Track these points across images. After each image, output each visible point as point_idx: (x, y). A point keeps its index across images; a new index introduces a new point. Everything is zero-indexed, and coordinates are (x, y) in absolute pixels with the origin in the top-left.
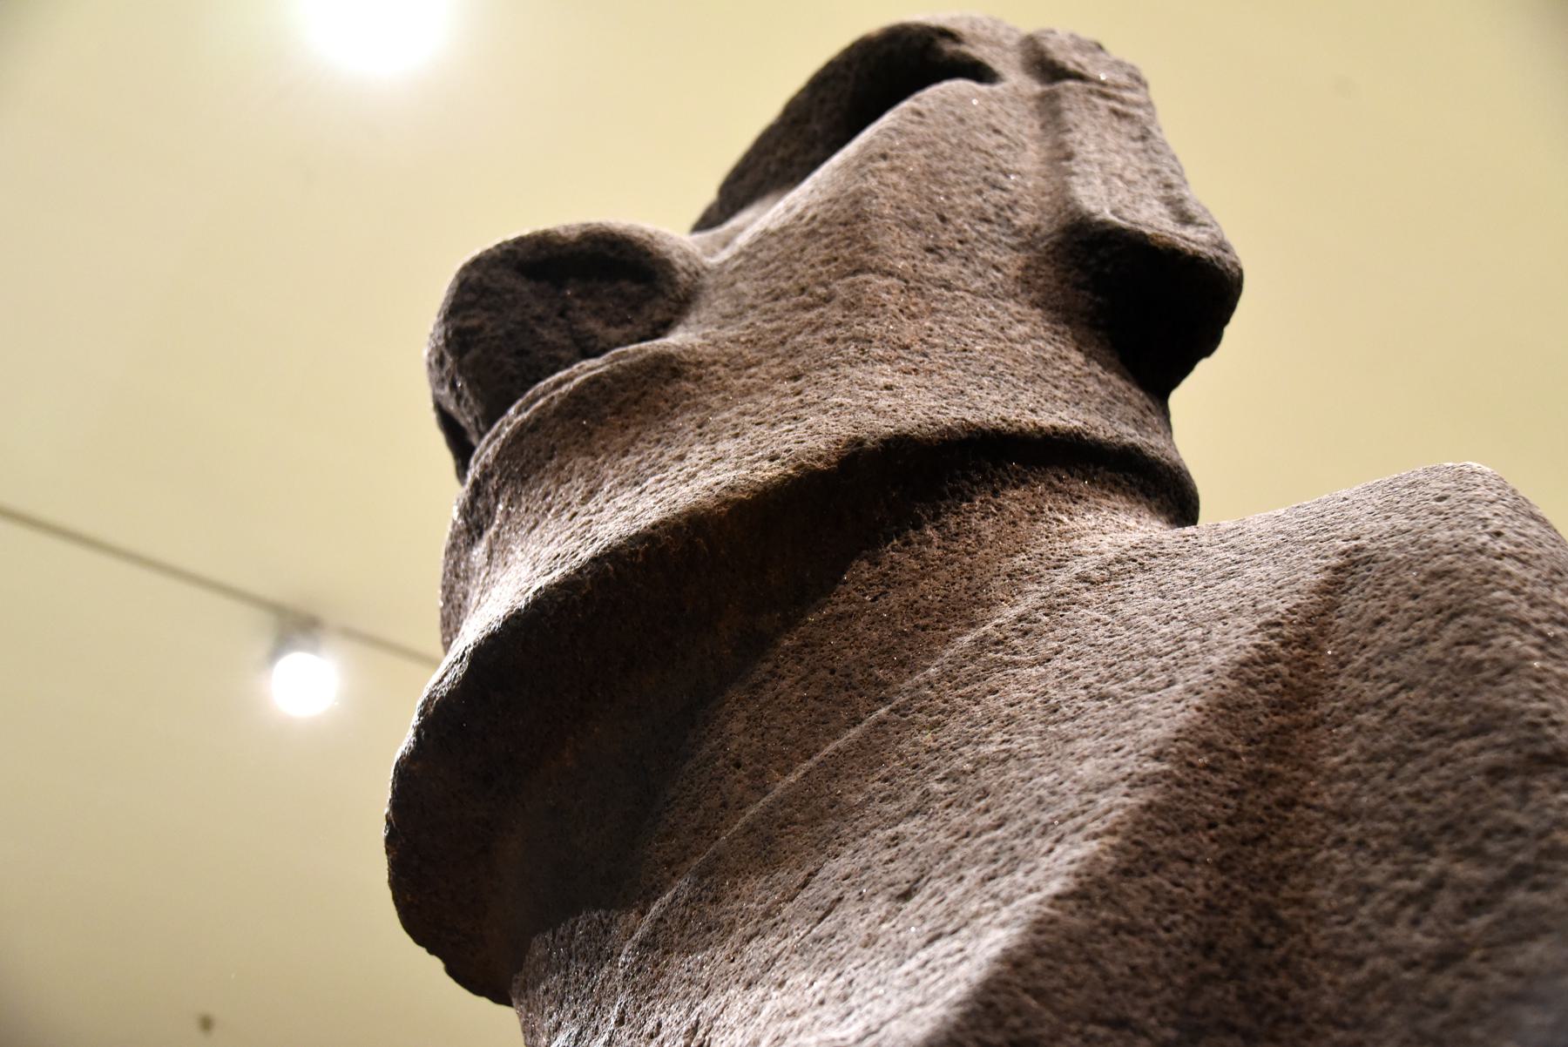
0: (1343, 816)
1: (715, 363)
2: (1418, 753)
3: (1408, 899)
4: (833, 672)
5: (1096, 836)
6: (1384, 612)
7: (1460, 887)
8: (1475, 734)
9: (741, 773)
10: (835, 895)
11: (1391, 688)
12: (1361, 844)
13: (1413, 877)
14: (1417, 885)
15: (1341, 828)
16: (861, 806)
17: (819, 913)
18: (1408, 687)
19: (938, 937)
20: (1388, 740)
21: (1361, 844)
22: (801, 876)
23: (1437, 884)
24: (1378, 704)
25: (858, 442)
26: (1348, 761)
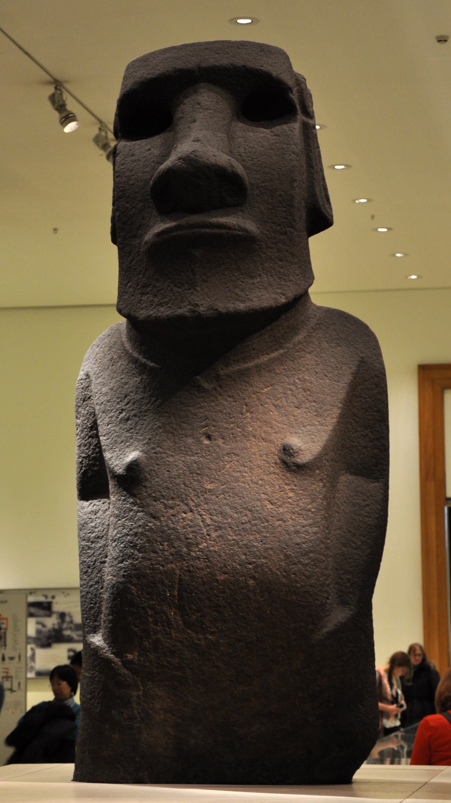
0: (355, 415)
1: (262, 241)
3: (362, 435)
4: (274, 337)
5: (334, 418)
6: (367, 379)
9: (254, 352)
10: (279, 396)
11: (367, 396)
12: (357, 422)
13: (364, 432)
14: (364, 434)
15: (355, 417)
16: (279, 374)
18: (369, 398)
19: (309, 425)
21: (357, 422)
23: (367, 435)
25: (296, 296)
26: (358, 406)
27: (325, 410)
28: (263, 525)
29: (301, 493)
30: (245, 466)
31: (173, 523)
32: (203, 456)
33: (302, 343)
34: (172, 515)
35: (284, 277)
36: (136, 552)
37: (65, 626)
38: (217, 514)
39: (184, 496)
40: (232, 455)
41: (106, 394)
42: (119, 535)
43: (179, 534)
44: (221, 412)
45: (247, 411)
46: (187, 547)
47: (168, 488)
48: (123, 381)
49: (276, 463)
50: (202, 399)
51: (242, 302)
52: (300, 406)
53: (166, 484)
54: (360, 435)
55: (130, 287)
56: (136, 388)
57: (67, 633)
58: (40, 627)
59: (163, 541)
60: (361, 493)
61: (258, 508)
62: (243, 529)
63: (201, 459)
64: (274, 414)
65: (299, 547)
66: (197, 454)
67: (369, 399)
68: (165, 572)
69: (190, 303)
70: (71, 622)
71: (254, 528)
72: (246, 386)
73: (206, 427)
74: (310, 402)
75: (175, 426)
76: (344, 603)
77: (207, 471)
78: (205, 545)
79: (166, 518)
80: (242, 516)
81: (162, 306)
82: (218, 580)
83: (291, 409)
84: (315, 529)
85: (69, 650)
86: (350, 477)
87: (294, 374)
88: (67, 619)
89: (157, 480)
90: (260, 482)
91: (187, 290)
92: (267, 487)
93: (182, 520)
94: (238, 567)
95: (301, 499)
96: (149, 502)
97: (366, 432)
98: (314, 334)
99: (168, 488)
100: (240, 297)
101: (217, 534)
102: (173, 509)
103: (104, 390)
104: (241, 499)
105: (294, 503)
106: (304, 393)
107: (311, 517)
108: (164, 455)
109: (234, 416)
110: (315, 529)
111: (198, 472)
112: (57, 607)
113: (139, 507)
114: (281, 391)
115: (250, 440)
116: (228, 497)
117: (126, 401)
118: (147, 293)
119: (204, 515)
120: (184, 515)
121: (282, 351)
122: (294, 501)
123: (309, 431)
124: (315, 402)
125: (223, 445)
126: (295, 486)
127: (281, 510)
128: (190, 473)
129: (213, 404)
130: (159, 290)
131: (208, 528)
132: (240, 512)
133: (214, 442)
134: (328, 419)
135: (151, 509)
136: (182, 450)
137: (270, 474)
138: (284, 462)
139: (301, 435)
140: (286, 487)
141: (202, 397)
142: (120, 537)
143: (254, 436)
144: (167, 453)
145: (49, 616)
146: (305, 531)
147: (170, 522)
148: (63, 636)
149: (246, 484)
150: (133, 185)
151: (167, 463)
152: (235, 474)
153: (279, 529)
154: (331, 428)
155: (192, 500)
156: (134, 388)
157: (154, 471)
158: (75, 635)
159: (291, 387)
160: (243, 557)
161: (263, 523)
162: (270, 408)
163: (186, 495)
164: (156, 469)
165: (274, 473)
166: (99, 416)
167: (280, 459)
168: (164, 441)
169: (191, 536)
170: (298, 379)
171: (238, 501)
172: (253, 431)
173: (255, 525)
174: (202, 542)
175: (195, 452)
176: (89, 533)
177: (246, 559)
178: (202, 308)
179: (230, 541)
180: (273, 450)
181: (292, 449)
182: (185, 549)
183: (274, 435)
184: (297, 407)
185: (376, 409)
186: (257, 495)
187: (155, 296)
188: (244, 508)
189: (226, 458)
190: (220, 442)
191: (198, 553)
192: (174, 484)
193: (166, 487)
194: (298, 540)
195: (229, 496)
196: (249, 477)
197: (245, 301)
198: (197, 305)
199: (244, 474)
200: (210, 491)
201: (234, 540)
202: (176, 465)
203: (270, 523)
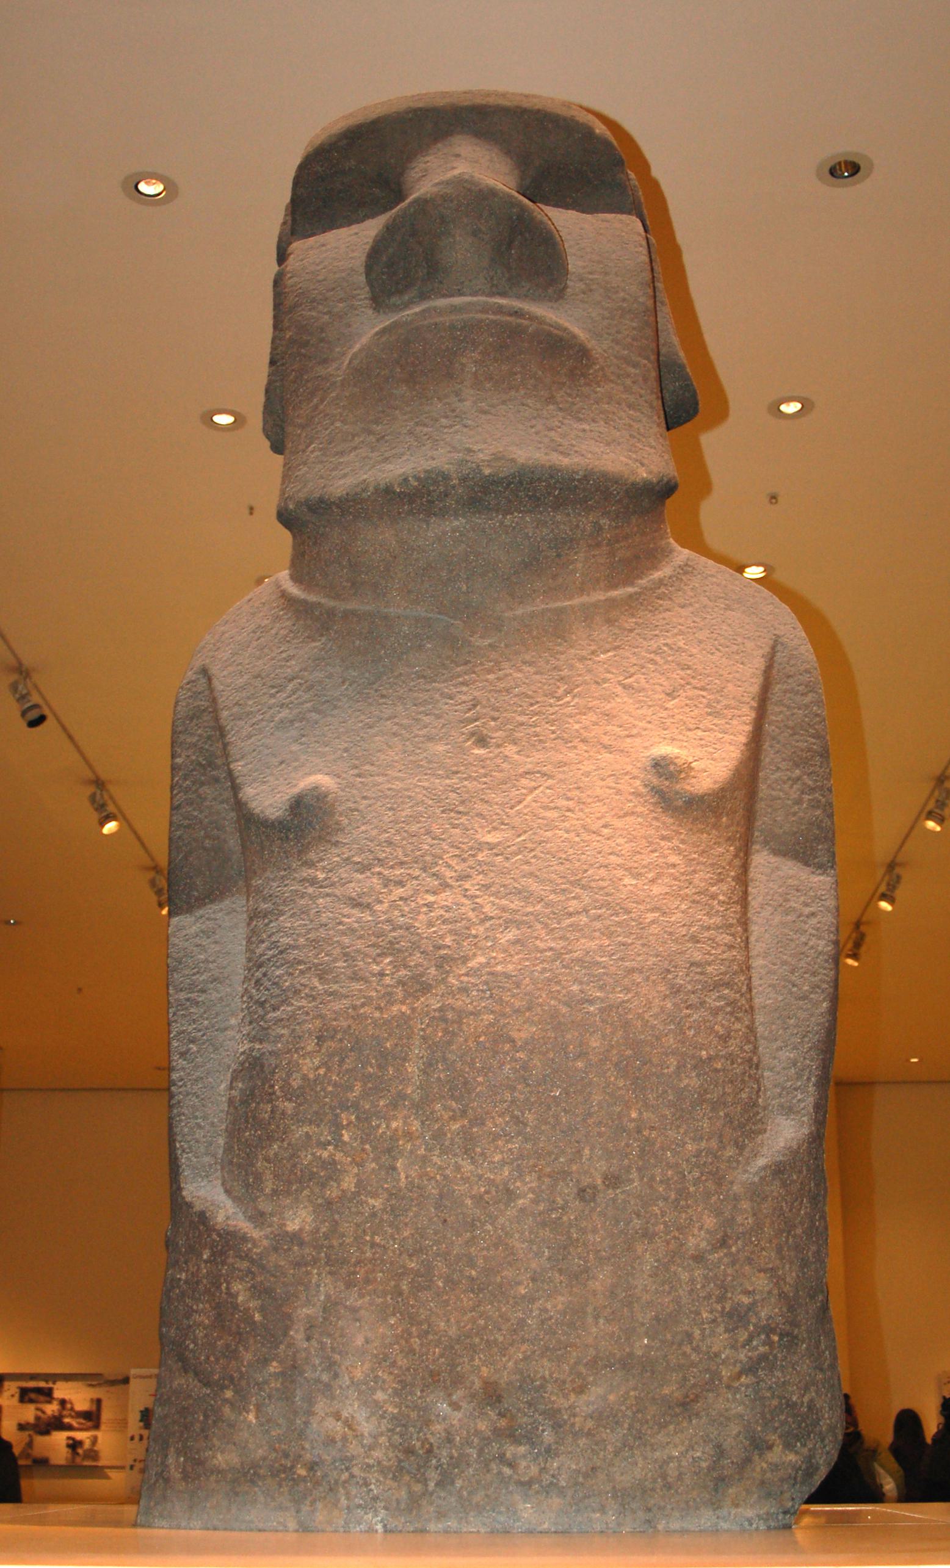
2: (798, 734)
5: (746, 724)
7: (805, 784)
8: (814, 738)
10: (632, 670)
17: (628, 675)
18: (799, 709)
19: (698, 728)
20: (790, 723)
22: (608, 646)
23: (798, 779)
24: (788, 707)
26: (777, 721)
27: (727, 707)
28: (617, 919)
29: (694, 859)
30: (569, 799)
31: (402, 916)
32: (470, 777)
33: (666, 585)
34: (401, 899)
35: (641, 438)
36: (316, 982)
37: (65, 1413)
38: (507, 894)
39: (428, 858)
40: (538, 775)
41: (243, 688)
42: (271, 953)
43: (416, 938)
44: (508, 691)
45: (567, 692)
46: (439, 967)
47: (389, 843)
48: (284, 655)
49: (638, 794)
50: (467, 667)
51: (565, 454)
52: (676, 694)
53: (387, 835)
54: (786, 778)
55: (312, 452)
56: (314, 660)
57: (67, 1420)
58: (39, 1413)
59: (378, 955)
60: (798, 890)
61: (604, 884)
62: (571, 926)
63: (466, 783)
64: (623, 702)
65: (699, 970)
66: (457, 772)
67: (796, 711)
68: (386, 1022)
69: (454, 447)
70: (72, 1409)
71: (598, 925)
72: (560, 645)
73: (476, 720)
74: (696, 688)
75: (405, 722)
76: (789, 1110)
77: (479, 807)
78: (482, 960)
79: (386, 905)
80: (568, 899)
81: (390, 463)
82: (513, 1041)
83: (656, 696)
84: (728, 939)
85: (69, 1438)
86: (774, 860)
87: (656, 635)
88: (69, 1406)
89: (363, 828)
90: (606, 831)
91: (446, 427)
92: (621, 841)
93: (425, 909)
94: (564, 1010)
95: (695, 872)
96: (344, 876)
97: (798, 772)
98: (684, 578)
99: (391, 843)
100: (560, 445)
101: (511, 934)
102: (403, 886)
103: (241, 681)
104: (562, 863)
105: (683, 878)
106: (682, 673)
107: (718, 911)
108: (380, 779)
109: (539, 700)
110: (728, 939)
111: (461, 809)
112: (58, 1394)
113: (321, 887)
114: (635, 662)
115: (575, 747)
116: (533, 860)
117: (290, 686)
118: (355, 448)
119: (477, 897)
120: (431, 898)
121: (630, 590)
122: (683, 874)
123: (701, 739)
124: (703, 689)
125: (516, 757)
126: (683, 842)
127: (656, 890)
128: (443, 812)
129: (491, 677)
130: (383, 437)
131: (488, 924)
132: (564, 890)
133: (497, 751)
134: (734, 722)
135: (352, 890)
136: (422, 766)
137: (626, 815)
138: (656, 791)
139: (685, 744)
140: (663, 843)
141: (466, 663)
142: (274, 956)
143: (584, 741)
144: (386, 775)
145: (50, 1402)
146: (710, 939)
147: (396, 913)
148: (62, 1423)
149: (573, 834)
150: (324, 280)
151: (389, 793)
152: (549, 814)
153: (654, 929)
154: (743, 739)
155: (449, 866)
156: (310, 661)
157: (357, 810)
158: (74, 1423)
159: (652, 656)
160: (575, 988)
161: (617, 915)
162: (615, 690)
163: (433, 856)
164: (361, 807)
165: (633, 813)
166: (228, 727)
167: (646, 786)
168: (379, 751)
169: (448, 941)
170: (666, 645)
171: (556, 868)
172: (582, 731)
173: (599, 917)
174: (475, 955)
175: (454, 769)
176: (194, 974)
177: (582, 991)
178: (481, 455)
179: (542, 951)
180: (629, 768)
181: (672, 763)
182: (433, 971)
183: (628, 740)
184: (668, 694)
185: (814, 731)
186: (599, 856)
187: (373, 449)
188: (571, 883)
189: (524, 782)
190: (510, 750)
191: (465, 979)
192: (405, 835)
193: (385, 841)
194: (698, 956)
195: (534, 857)
196: (578, 819)
197: (569, 454)
198: (469, 450)
199: (568, 814)
200: (491, 847)
201: (551, 949)
202: (409, 797)
203: (633, 915)
